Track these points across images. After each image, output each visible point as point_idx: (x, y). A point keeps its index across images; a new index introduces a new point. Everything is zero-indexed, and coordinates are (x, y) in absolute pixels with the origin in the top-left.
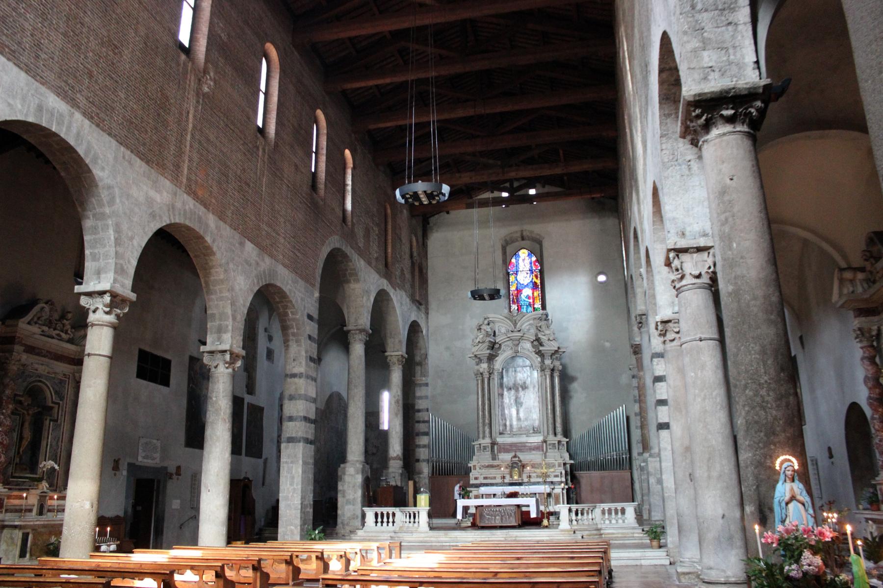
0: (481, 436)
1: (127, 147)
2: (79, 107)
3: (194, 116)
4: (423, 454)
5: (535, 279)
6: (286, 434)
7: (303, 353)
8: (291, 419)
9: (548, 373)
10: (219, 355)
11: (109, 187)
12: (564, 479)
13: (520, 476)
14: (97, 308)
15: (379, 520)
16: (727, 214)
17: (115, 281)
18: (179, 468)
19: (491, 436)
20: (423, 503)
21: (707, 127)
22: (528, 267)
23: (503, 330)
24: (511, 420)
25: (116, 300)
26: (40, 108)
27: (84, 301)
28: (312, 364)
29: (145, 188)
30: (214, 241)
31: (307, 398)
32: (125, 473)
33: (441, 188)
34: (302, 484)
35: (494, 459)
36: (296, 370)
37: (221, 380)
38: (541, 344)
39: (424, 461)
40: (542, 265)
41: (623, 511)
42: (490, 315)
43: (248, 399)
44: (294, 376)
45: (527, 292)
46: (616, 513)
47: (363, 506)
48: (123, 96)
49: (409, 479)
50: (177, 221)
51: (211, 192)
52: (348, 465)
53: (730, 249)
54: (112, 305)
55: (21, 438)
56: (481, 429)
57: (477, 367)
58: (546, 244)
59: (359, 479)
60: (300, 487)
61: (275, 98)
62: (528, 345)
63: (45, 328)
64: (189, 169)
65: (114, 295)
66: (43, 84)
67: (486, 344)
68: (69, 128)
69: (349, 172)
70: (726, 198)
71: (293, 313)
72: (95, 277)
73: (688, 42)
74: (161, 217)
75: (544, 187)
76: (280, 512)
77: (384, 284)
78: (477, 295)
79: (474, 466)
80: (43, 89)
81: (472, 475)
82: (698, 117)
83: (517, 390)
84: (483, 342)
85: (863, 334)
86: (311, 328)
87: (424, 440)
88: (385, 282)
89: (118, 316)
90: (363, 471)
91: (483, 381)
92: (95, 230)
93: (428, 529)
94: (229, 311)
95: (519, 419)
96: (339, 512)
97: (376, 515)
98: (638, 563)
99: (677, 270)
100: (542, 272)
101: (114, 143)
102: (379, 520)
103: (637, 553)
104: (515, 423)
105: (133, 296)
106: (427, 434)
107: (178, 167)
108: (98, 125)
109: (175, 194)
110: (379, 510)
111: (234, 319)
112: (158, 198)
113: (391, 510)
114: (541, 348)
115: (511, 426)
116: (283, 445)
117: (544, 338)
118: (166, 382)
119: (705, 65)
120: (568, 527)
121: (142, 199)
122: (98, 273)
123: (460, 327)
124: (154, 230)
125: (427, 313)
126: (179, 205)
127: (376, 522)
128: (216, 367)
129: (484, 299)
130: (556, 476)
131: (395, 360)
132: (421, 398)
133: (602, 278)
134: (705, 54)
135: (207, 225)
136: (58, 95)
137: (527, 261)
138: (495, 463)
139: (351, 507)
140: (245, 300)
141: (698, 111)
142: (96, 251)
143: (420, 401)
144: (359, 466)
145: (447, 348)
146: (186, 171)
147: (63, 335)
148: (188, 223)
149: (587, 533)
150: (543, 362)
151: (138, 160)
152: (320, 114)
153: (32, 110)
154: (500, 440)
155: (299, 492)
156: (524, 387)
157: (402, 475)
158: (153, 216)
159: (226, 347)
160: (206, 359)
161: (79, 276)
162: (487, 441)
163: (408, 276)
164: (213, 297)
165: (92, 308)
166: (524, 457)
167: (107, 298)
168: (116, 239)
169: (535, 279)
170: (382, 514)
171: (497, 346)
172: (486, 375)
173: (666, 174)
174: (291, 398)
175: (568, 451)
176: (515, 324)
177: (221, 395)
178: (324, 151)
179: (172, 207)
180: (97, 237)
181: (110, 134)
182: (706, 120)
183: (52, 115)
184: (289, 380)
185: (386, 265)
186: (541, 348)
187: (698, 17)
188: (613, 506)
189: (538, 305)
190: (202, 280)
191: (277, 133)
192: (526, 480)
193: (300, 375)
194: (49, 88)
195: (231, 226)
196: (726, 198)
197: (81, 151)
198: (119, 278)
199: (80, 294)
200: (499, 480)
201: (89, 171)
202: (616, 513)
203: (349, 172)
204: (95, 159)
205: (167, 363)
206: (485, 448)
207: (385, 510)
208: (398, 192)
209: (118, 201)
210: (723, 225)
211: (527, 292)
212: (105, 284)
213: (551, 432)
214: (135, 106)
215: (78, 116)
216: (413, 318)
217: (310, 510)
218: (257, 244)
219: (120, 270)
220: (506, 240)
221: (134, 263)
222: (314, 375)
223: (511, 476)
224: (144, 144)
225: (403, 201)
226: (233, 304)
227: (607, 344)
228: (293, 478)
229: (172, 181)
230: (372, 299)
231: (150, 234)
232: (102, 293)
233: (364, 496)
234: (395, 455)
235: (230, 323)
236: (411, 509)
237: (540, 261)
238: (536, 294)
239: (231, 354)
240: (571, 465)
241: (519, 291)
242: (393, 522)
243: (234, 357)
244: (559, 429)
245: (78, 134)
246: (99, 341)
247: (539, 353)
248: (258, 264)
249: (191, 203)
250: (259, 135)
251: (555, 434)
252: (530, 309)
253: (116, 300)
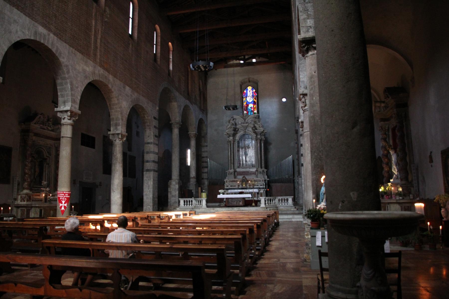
1: (73, 47)
2: (52, 31)
3: (101, 32)
4: (205, 176)
5: (254, 100)
6: (145, 168)
7: (152, 134)
8: (147, 161)
9: (259, 141)
10: (116, 135)
11: (67, 66)
12: (264, 187)
13: (246, 185)
14: (65, 118)
15: (186, 203)
16: (313, 86)
17: (72, 106)
18: (100, 183)
19: (234, 168)
20: (204, 196)
21: (307, 51)
22: (251, 95)
23: (240, 123)
24: (243, 161)
25: (72, 114)
26: (36, 33)
27: (59, 115)
28: (156, 138)
29: (82, 65)
30: (112, 87)
31: (154, 153)
32: (78, 185)
33: (209, 64)
34: (153, 188)
35: (235, 178)
36: (149, 141)
37: (118, 146)
38: (257, 129)
39: (205, 179)
40: (258, 94)
41: (287, 200)
42: (234, 116)
43: (129, 153)
44: (148, 143)
45: (251, 105)
46: (285, 201)
47: (179, 198)
48: (70, 25)
49: (199, 187)
50: (96, 79)
51: (110, 65)
52: (172, 181)
53: (313, 99)
54: (71, 116)
55: (35, 172)
56: (230, 165)
57: (228, 139)
58: (260, 84)
59: (177, 186)
60: (152, 190)
61: (136, 21)
62: (251, 129)
63: (42, 125)
64: (100, 55)
65: (72, 112)
66: (36, 22)
67: (232, 128)
68: (48, 41)
69: (171, 52)
70: (313, 80)
71: (147, 116)
72: (63, 104)
73: (302, 15)
74: (89, 78)
75: (259, 58)
76: (144, 200)
77: (188, 102)
78: (227, 108)
80: (36, 24)
81: (226, 184)
82: (304, 47)
83: (245, 149)
84: (231, 128)
85: (382, 129)
86: (155, 123)
87: (206, 170)
88: (188, 101)
89: (74, 121)
90: (179, 183)
91: (231, 145)
92: (61, 84)
93: (206, 207)
94: (120, 117)
95: (246, 161)
96: (169, 200)
97: (184, 202)
98: (291, 220)
99: (303, 102)
100: (257, 96)
101: (68, 46)
102: (186, 203)
103: (290, 217)
104: (244, 162)
105: (80, 112)
106: (207, 167)
107: (95, 55)
108: (60, 39)
109: (95, 67)
110: (186, 199)
111: (122, 120)
112: (88, 69)
113: (190, 199)
114: (256, 131)
115: (243, 164)
116: (144, 173)
117: (257, 126)
118: (93, 146)
119: (308, 25)
120: (264, 206)
121: (81, 70)
122: (64, 102)
124: (87, 83)
125: (207, 115)
126: (97, 72)
127: (185, 204)
128: (115, 141)
129: (230, 110)
130: (261, 185)
131: (192, 135)
132: (204, 152)
133: (284, 100)
134: (308, 21)
135: (109, 80)
136: (43, 26)
137: (251, 92)
138: (236, 180)
139: (174, 198)
140: (126, 112)
141: (304, 45)
142: (63, 93)
143: (204, 153)
144: (177, 181)
145: (216, 130)
146: (99, 57)
147: (49, 128)
148: (101, 79)
149: (272, 208)
150: (257, 136)
151: (78, 53)
152: (157, 27)
153: (32, 34)
154: (238, 170)
155: (152, 192)
156: (249, 147)
157: (196, 185)
158: (86, 77)
159: (119, 132)
160: (111, 137)
161: (56, 104)
162: (232, 170)
163: (198, 98)
164: (113, 110)
165: (63, 117)
166: (247, 177)
167: (69, 114)
168: (71, 88)
169: (254, 100)
170: (187, 201)
171: (237, 129)
172: (232, 142)
173: (301, 62)
174: (148, 153)
175: (267, 175)
176: (245, 120)
177: (118, 152)
178: (159, 44)
179: (94, 73)
180: (63, 87)
181: (65, 42)
182: (307, 48)
183: (41, 36)
184: (146, 145)
185: (188, 94)
186: (256, 131)
187: (307, 5)
188: (283, 197)
189: (256, 111)
190: (108, 104)
191: (138, 37)
192: (248, 187)
193: (151, 143)
194: (39, 23)
195: (119, 80)
196: (313, 80)
197: (54, 50)
198: (73, 104)
199: (57, 112)
200: (237, 187)
201: (58, 59)
202: (285, 201)
203: (171, 52)
204: (60, 53)
205: (94, 139)
206: (231, 173)
207: (188, 199)
208: (191, 65)
209: (71, 71)
210: (310, 90)
211: (251, 105)
212: (68, 108)
213: (259, 167)
214: (75, 29)
215: (52, 35)
216: (201, 116)
217: (157, 199)
218: (131, 87)
219: (73, 101)
220: (242, 83)
221: (79, 98)
222: (157, 143)
223: (242, 185)
224: (80, 46)
225: (193, 69)
226: (121, 114)
227: (285, 129)
228: (149, 186)
229: (93, 62)
230: (182, 109)
231: (85, 85)
232: (66, 111)
233: (179, 193)
234: (193, 176)
235: (120, 122)
236: (199, 199)
237: (257, 91)
238: (255, 106)
239: (122, 135)
240: (268, 181)
241: (247, 105)
242: (192, 204)
243: (123, 136)
244: (263, 165)
245: (52, 43)
246: (67, 131)
247: (255, 132)
248: (131, 96)
249: (102, 71)
250: (130, 38)
251: (261, 168)
252: (252, 113)
253: (72, 114)
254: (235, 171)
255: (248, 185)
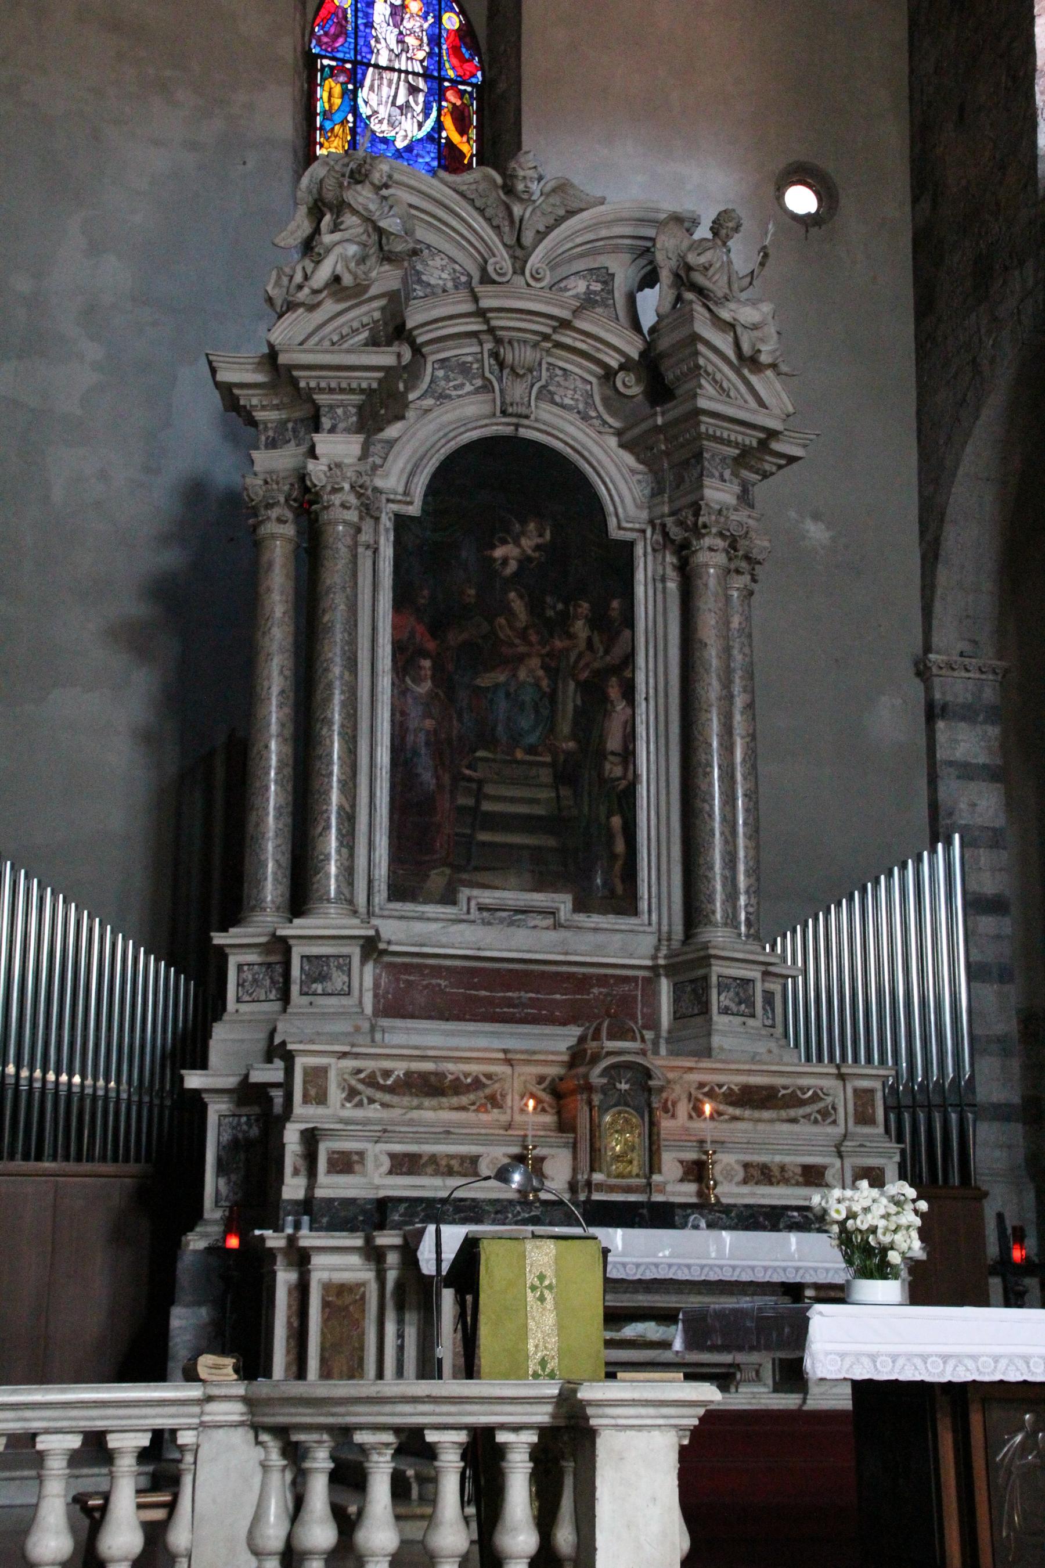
0: (271, 883)
5: (450, 132)
67: (370, 311)
79: (317, 1076)
84: (356, 293)
123: (22, 284)
133: (801, 200)
170: (95, 1449)
206: (318, 969)
227: (816, 532)
254: (371, 947)
255: (671, 1165)
